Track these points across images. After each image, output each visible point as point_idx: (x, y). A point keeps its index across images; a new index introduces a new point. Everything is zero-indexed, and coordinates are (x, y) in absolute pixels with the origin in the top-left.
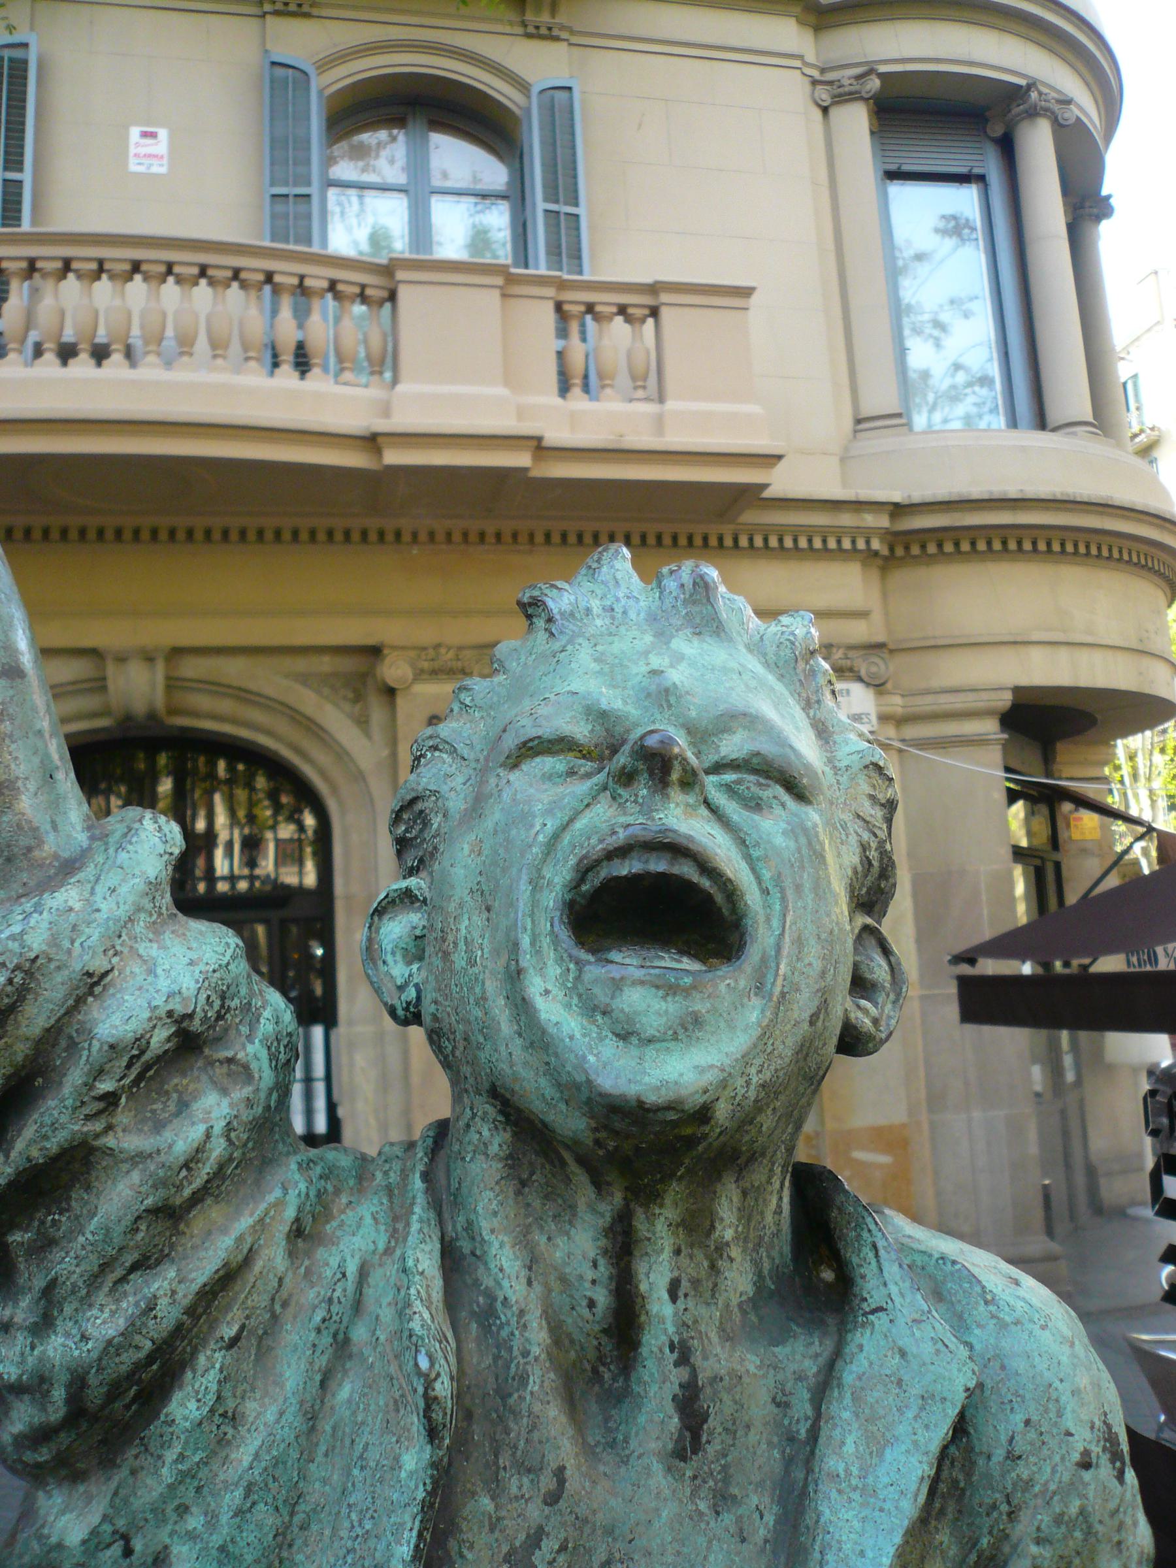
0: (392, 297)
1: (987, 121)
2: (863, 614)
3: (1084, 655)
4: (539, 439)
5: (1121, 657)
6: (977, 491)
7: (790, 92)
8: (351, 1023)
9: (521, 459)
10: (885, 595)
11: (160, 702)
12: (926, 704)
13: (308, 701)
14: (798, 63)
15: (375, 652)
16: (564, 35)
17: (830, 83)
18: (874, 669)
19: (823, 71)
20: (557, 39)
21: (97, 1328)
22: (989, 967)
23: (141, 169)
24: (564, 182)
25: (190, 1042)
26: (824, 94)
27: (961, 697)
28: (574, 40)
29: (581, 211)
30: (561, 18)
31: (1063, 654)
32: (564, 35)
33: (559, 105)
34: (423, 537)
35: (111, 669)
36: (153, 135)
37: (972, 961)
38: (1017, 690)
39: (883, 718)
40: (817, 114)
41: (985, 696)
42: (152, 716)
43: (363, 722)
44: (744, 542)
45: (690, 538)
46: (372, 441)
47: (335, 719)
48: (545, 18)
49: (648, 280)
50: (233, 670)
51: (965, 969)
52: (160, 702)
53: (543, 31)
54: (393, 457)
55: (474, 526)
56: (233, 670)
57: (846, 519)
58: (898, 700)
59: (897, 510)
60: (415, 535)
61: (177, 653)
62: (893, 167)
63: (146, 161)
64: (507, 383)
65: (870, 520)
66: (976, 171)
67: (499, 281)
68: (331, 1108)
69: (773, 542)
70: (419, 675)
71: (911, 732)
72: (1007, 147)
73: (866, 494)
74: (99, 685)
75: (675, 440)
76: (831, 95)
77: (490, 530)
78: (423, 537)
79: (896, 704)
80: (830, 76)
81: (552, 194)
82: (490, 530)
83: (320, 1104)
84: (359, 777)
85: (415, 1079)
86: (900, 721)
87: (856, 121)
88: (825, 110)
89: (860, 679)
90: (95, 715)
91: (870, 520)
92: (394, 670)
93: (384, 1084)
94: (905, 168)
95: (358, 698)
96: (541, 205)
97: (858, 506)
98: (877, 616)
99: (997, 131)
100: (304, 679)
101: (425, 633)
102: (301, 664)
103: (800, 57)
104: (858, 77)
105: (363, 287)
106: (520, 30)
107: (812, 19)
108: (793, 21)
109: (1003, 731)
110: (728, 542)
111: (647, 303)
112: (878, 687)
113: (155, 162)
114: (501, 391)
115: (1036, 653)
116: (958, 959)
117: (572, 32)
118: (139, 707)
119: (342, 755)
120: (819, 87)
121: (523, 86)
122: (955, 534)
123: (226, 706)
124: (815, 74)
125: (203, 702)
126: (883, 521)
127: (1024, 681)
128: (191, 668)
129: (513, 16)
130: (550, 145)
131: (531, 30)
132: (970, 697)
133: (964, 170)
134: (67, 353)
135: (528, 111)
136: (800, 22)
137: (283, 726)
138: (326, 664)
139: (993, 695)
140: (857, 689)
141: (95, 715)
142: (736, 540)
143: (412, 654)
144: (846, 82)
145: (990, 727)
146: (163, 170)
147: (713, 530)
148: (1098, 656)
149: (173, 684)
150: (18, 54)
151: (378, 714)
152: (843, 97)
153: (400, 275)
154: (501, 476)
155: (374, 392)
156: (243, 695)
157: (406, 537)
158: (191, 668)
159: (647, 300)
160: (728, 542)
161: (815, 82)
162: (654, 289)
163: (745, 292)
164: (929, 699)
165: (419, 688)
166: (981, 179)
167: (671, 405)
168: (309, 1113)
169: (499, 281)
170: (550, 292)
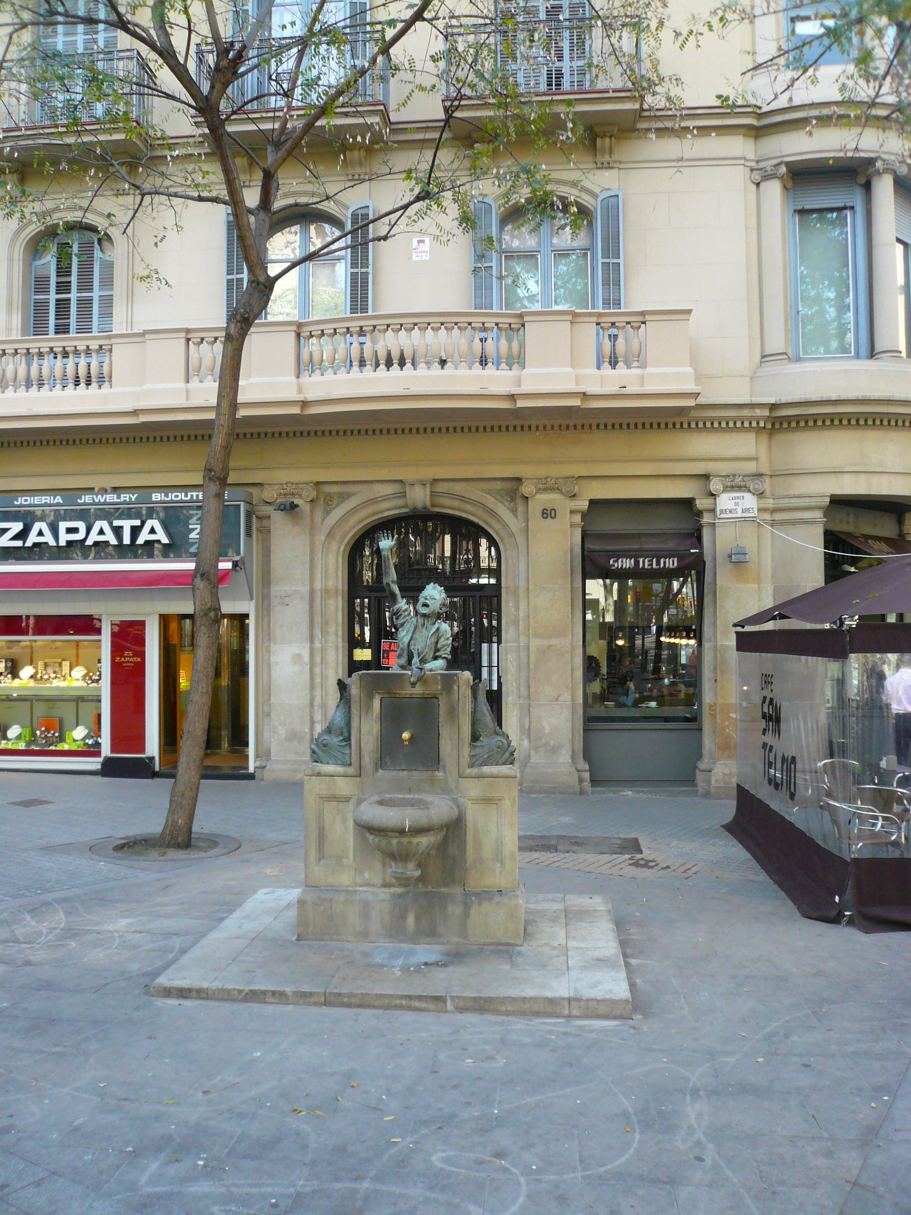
0: (523, 325)
1: (858, 174)
2: (756, 459)
3: (876, 479)
4: (584, 394)
5: (900, 477)
6: (814, 397)
7: (736, 179)
8: (506, 642)
9: (577, 402)
10: (770, 447)
11: (428, 503)
12: (784, 503)
13: (490, 501)
14: (742, 162)
15: (519, 480)
16: (615, 165)
17: (761, 169)
18: (756, 487)
19: (758, 162)
20: (613, 168)
21: (402, 621)
22: (748, 629)
23: (418, 259)
24: (612, 247)
25: (406, 610)
26: (757, 176)
27: (804, 500)
28: (621, 166)
29: (621, 261)
30: (615, 157)
31: (863, 477)
32: (615, 165)
33: (612, 207)
34: (541, 428)
35: (408, 489)
36: (423, 241)
37: (743, 627)
38: (832, 496)
39: (759, 510)
40: (754, 187)
41: (815, 499)
42: (425, 508)
43: (514, 511)
44: (693, 425)
45: (666, 424)
46: (512, 397)
47: (503, 510)
48: (607, 158)
49: (641, 310)
50: (458, 488)
51: (739, 629)
52: (428, 503)
53: (606, 165)
54: (521, 404)
55: (564, 423)
56: (458, 488)
57: (746, 413)
58: (771, 501)
59: (773, 407)
60: (537, 427)
61: (435, 481)
62: (800, 208)
63: (420, 254)
64: (572, 366)
65: (758, 412)
66: (849, 204)
67: (570, 318)
68: (499, 678)
69: (708, 425)
70: (539, 491)
71: (778, 516)
72: (867, 187)
73: (756, 400)
74: (403, 495)
75: (649, 388)
76: (761, 176)
77: (571, 424)
78: (541, 428)
79: (769, 503)
80: (762, 165)
81: (606, 255)
82: (571, 424)
83: (495, 677)
84: (513, 535)
85: (532, 667)
86: (773, 511)
87: (774, 190)
88: (758, 185)
89: (750, 491)
90: (400, 507)
91: (758, 412)
92: (527, 489)
93: (519, 669)
94: (807, 207)
95: (513, 500)
96: (600, 260)
97: (752, 406)
98: (764, 459)
99: (862, 180)
100: (489, 492)
101: (542, 471)
102: (487, 486)
103: (745, 159)
104: (776, 166)
105: (510, 324)
106: (594, 166)
107: (753, 133)
108: (741, 137)
109: (825, 517)
110: (685, 425)
111: (642, 318)
112: (761, 495)
113: (424, 254)
114: (569, 370)
115: (847, 478)
116: (735, 625)
117: (620, 162)
118: (420, 505)
119: (505, 525)
120: (754, 172)
121: (595, 196)
122: (806, 418)
123: (456, 503)
124: (753, 164)
125: (446, 501)
126: (766, 413)
127: (839, 491)
128: (441, 488)
129: (589, 158)
130: (606, 227)
131: (599, 165)
132: (808, 500)
133: (841, 205)
134: (389, 364)
135: (596, 209)
136: (744, 135)
137: (480, 512)
138: (498, 485)
139: (820, 499)
140: (748, 496)
141: (400, 507)
142: (689, 424)
143: (535, 481)
144: (769, 169)
145: (818, 515)
146: (428, 258)
147: (678, 421)
148: (885, 478)
149: (433, 494)
150: (364, 211)
151: (521, 508)
152: (767, 177)
153: (526, 319)
154: (570, 409)
155: (515, 372)
156: (462, 499)
157: (534, 428)
158: (441, 488)
159: (640, 319)
160: (685, 425)
161: (752, 170)
162: (643, 313)
163: (689, 312)
164: (786, 500)
165: (537, 496)
166: (852, 208)
167: (649, 370)
168: (490, 680)
169: (570, 318)
170: (595, 319)
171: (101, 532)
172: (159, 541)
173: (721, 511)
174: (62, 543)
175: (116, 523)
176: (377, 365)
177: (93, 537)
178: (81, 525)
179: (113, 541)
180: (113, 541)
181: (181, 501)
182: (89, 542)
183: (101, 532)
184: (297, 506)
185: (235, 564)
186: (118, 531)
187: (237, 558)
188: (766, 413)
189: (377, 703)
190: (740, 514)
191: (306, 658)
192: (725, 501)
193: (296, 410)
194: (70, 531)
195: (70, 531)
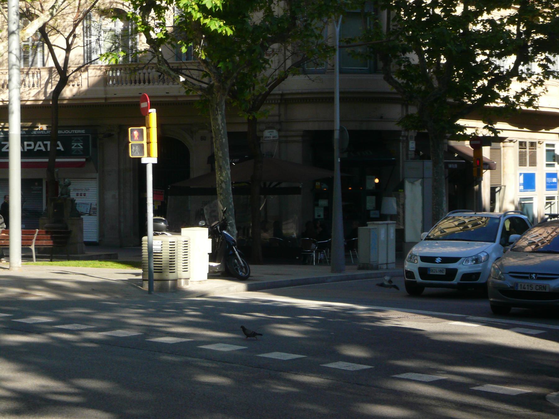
39: (280, 137)
65: (277, 97)
91: (277, 97)
126: (280, 97)
140: (275, 131)
171: (40, 146)
172: (60, 150)
173: (266, 137)
174: (26, 150)
175: (45, 142)
176: (131, 83)
177: (37, 148)
178: (32, 143)
179: (44, 150)
180: (44, 150)
181: (69, 134)
182: (35, 150)
183: (40, 146)
184: (113, 135)
185: (87, 159)
186: (45, 146)
187: (88, 157)
188: (280, 97)
189: (52, 204)
190: (272, 139)
191: (117, 197)
192: (267, 133)
193: (103, 101)
194: (28, 145)
195: (28, 145)
